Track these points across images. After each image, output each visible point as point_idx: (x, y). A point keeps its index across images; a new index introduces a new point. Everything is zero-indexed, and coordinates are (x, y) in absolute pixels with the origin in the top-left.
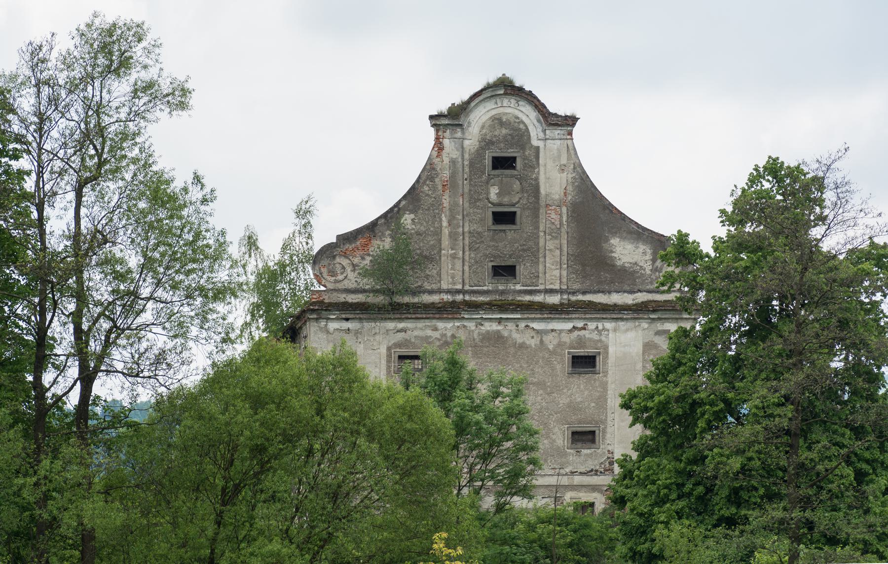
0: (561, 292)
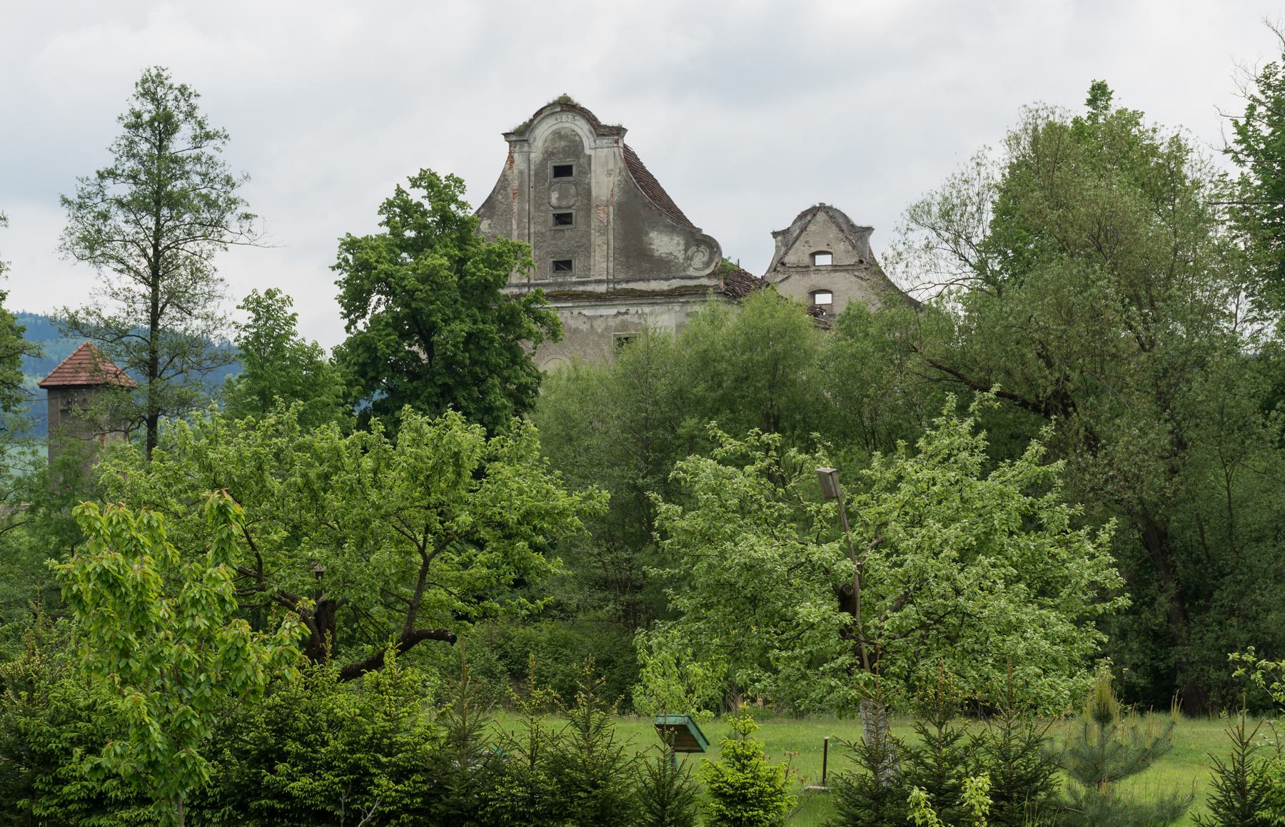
0: (608, 282)
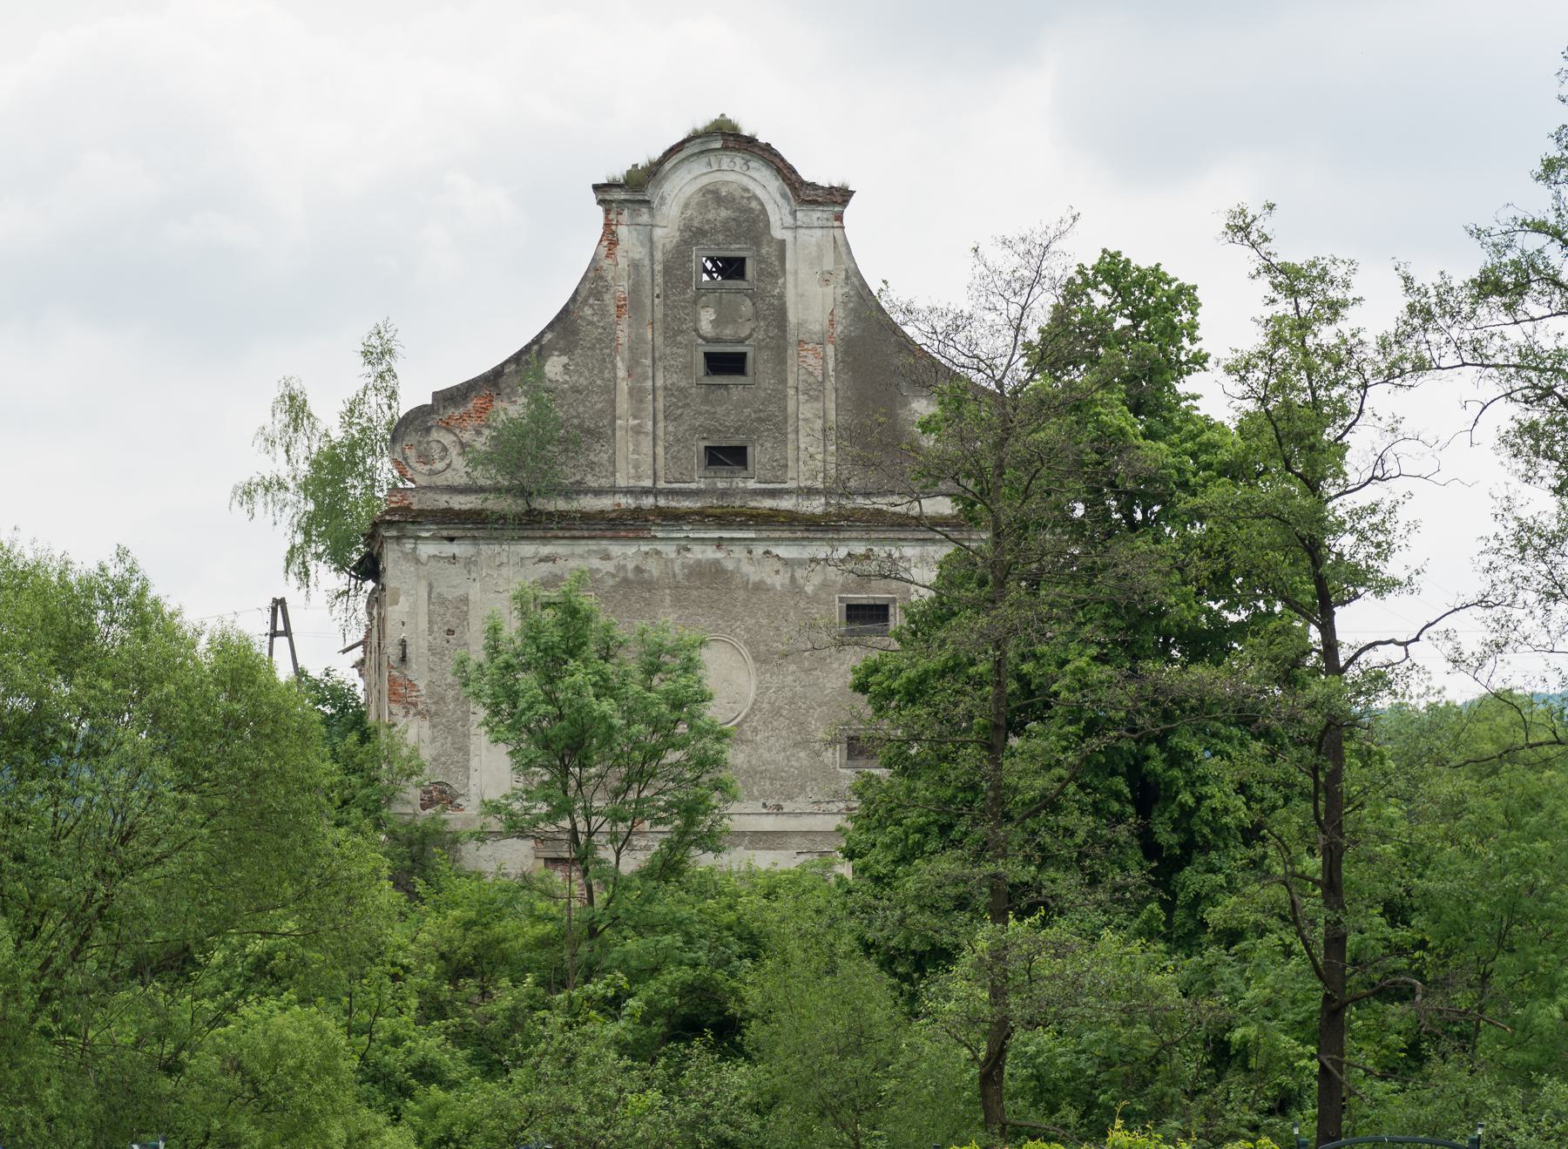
0: (827, 493)
